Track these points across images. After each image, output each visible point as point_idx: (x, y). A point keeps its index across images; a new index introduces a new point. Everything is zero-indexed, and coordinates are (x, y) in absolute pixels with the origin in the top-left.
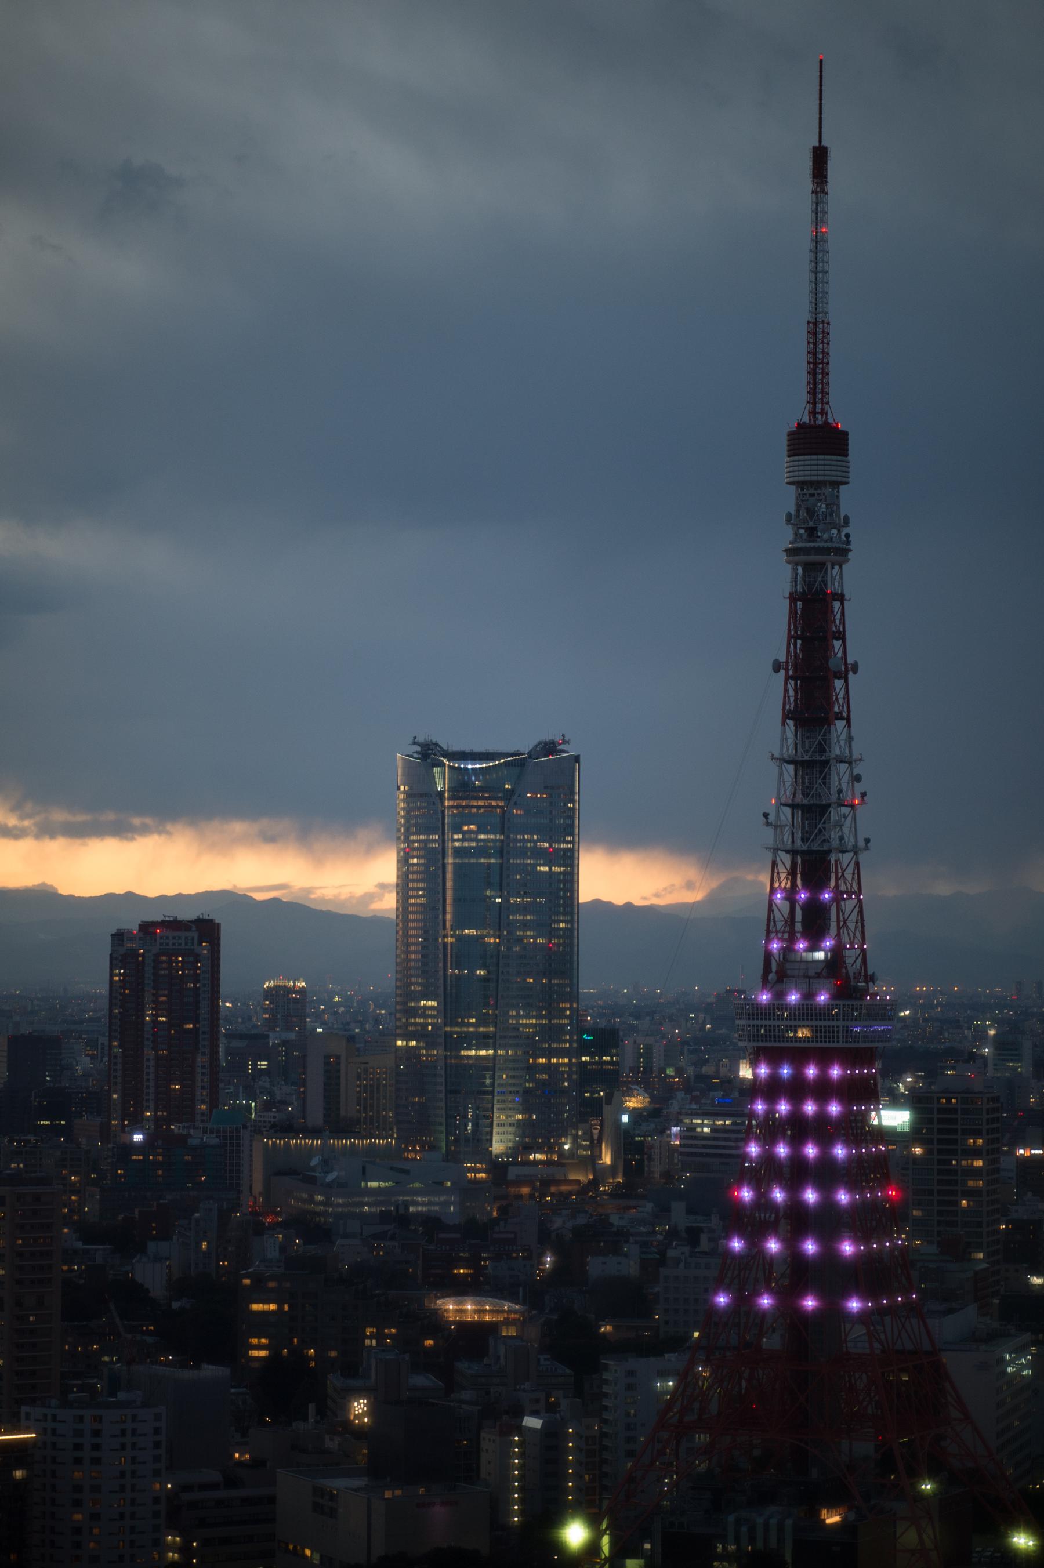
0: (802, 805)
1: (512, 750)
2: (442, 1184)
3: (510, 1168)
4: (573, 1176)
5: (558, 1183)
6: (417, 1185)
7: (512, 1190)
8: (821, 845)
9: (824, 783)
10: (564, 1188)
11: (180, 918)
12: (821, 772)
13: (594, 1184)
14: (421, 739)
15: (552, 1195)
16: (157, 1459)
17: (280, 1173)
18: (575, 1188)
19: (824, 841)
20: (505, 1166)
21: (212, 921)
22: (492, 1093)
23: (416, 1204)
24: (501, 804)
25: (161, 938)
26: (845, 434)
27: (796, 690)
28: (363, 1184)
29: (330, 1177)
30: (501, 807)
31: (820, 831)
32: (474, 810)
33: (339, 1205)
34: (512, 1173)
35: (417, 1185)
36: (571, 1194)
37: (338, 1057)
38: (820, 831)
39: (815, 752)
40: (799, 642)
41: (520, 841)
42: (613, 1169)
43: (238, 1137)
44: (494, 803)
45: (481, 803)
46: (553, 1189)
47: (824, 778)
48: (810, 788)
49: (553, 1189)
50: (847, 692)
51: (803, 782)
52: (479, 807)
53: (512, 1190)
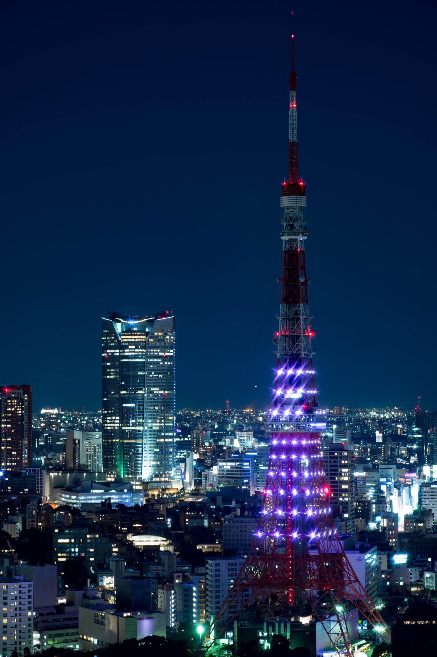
0: (290, 336)
5: (169, 489)
8: (297, 352)
9: (298, 327)
10: (172, 492)
12: (297, 323)
13: (183, 489)
17: (56, 487)
18: (175, 491)
19: (298, 350)
20: (147, 483)
21: (28, 386)
22: (142, 454)
23: (113, 499)
24: (144, 337)
25: (8, 393)
27: (286, 289)
28: (91, 491)
30: (145, 339)
31: (297, 346)
32: (133, 340)
33: (82, 500)
36: (174, 494)
37: (79, 440)
38: (297, 346)
39: (294, 314)
40: (287, 270)
41: (152, 352)
43: (41, 473)
44: (141, 337)
45: (136, 337)
47: (298, 325)
48: (292, 329)
50: (306, 291)
51: (289, 326)
52: (135, 339)
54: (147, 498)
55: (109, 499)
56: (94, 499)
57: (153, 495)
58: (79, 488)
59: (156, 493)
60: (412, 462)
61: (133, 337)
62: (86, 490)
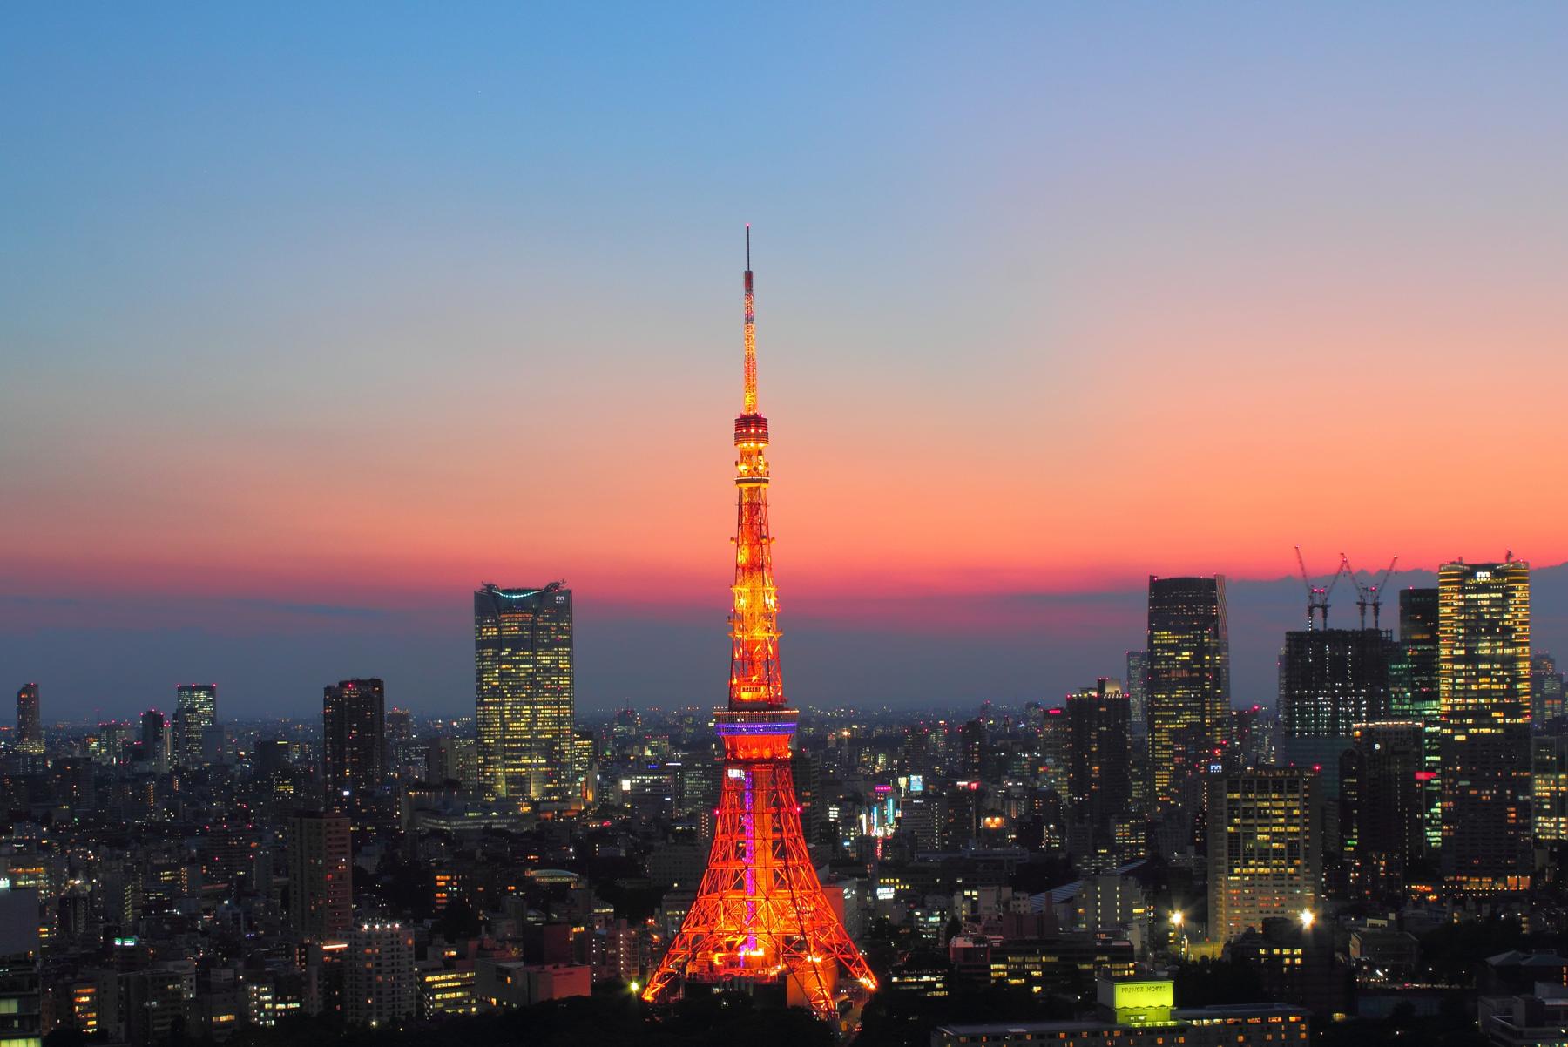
1: (536, 587)
2: (507, 813)
3: (541, 805)
4: (574, 808)
5: (566, 811)
6: (494, 814)
7: (542, 815)
10: (570, 814)
11: (361, 679)
14: (486, 583)
15: (564, 818)
16: (410, 956)
17: (418, 810)
18: (576, 813)
26: (766, 420)
29: (449, 811)
34: (542, 806)
35: (494, 814)
42: (594, 803)
45: (520, 616)
46: (564, 815)
49: (564, 815)
53: (542, 815)
54: (538, 822)
55: (491, 824)
56: (470, 825)
57: (547, 819)
58: (449, 811)
59: (549, 815)
60: (877, 771)
61: (517, 616)
62: (459, 814)
